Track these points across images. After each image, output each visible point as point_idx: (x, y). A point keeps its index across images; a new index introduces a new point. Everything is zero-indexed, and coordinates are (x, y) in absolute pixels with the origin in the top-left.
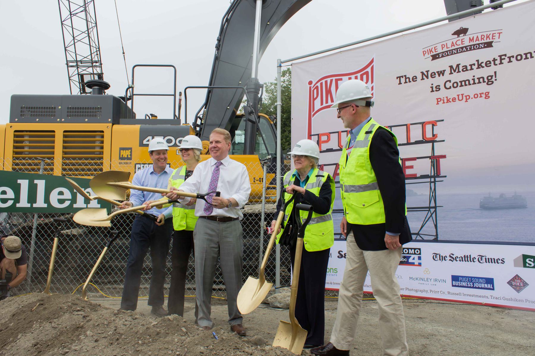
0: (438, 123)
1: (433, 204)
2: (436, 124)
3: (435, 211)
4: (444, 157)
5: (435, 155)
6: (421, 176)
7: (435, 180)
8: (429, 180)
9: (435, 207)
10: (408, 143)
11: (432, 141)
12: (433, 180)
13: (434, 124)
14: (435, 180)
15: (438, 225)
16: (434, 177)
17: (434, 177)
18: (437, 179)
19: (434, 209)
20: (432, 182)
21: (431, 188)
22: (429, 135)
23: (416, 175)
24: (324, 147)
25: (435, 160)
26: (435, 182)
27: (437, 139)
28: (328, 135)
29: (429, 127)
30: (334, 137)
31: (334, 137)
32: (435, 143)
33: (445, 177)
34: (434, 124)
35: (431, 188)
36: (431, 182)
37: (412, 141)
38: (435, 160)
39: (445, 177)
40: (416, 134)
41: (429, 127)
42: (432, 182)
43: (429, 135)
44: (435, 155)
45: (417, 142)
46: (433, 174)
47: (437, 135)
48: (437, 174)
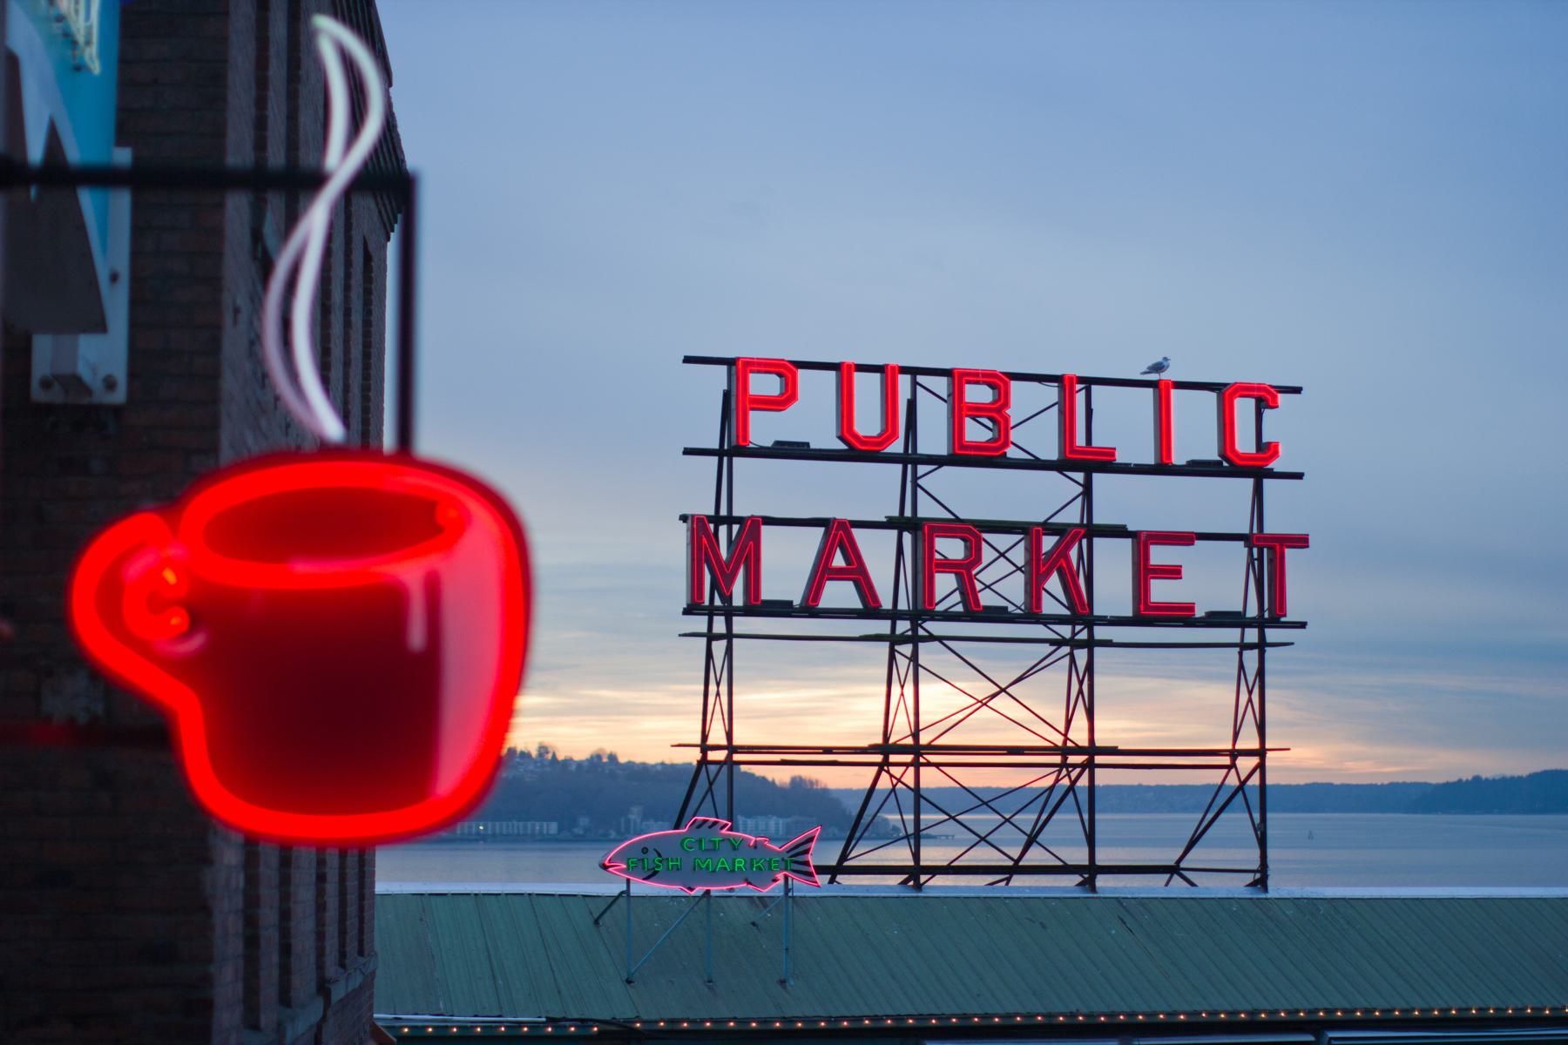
0: (1281, 398)
1: (1249, 741)
2: (1275, 398)
3: (1261, 766)
4: (1301, 542)
5: (1268, 530)
6: (1211, 615)
7: (1262, 636)
8: (1233, 635)
9: (1261, 753)
10: (1163, 467)
11: (1256, 468)
12: (1252, 635)
13: (1265, 398)
14: (1262, 636)
15: (1270, 832)
16: (1261, 624)
17: (1261, 624)
18: (1272, 635)
19: (1255, 761)
20: (1251, 646)
21: (1241, 667)
22: (1245, 443)
23: (1190, 607)
24: (763, 428)
25: (1269, 552)
26: (1262, 645)
27: (1276, 465)
28: (787, 370)
29: (1244, 408)
30: (817, 389)
31: (817, 389)
32: (1267, 483)
33: (1302, 625)
34: (1265, 398)
35: (1241, 667)
36: (1243, 646)
37: (1178, 458)
38: (1269, 552)
39: (1302, 625)
40: (1196, 435)
41: (1244, 408)
42: (1251, 646)
43: (1245, 443)
44: (1268, 530)
45: (1197, 469)
46: (1252, 611)
47: (1276, 445)
48: (1274, 614)
